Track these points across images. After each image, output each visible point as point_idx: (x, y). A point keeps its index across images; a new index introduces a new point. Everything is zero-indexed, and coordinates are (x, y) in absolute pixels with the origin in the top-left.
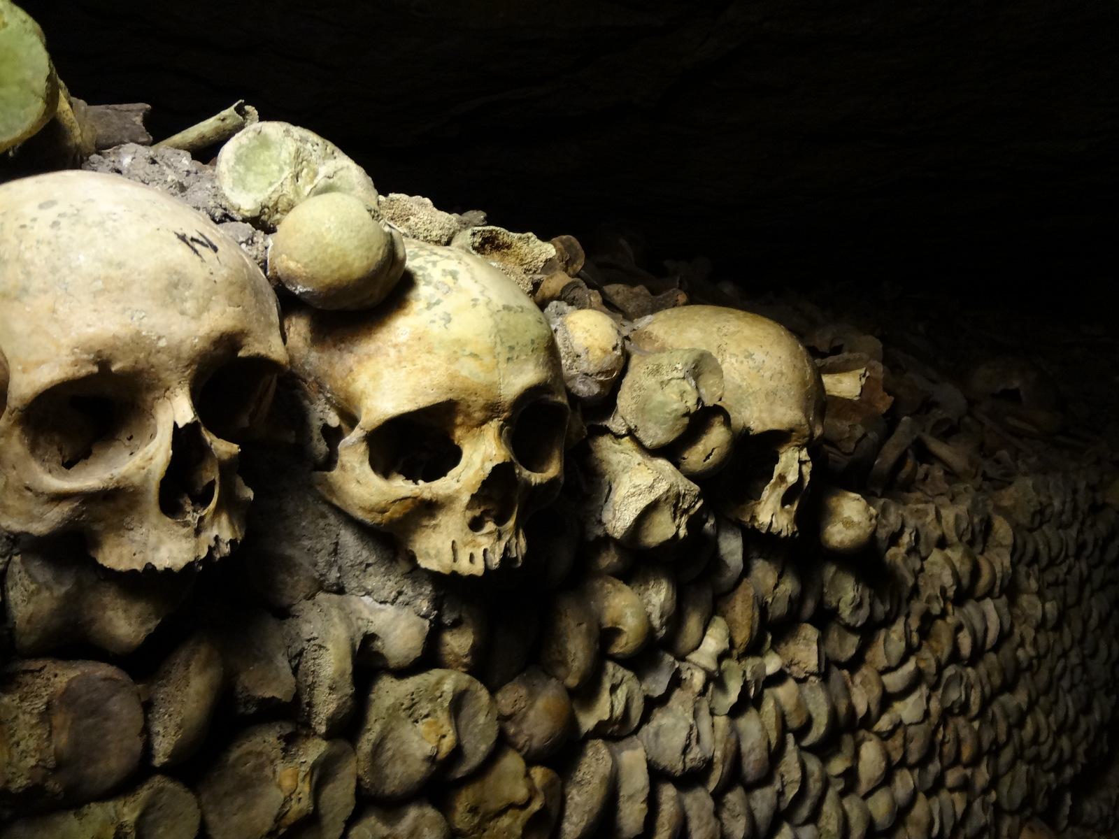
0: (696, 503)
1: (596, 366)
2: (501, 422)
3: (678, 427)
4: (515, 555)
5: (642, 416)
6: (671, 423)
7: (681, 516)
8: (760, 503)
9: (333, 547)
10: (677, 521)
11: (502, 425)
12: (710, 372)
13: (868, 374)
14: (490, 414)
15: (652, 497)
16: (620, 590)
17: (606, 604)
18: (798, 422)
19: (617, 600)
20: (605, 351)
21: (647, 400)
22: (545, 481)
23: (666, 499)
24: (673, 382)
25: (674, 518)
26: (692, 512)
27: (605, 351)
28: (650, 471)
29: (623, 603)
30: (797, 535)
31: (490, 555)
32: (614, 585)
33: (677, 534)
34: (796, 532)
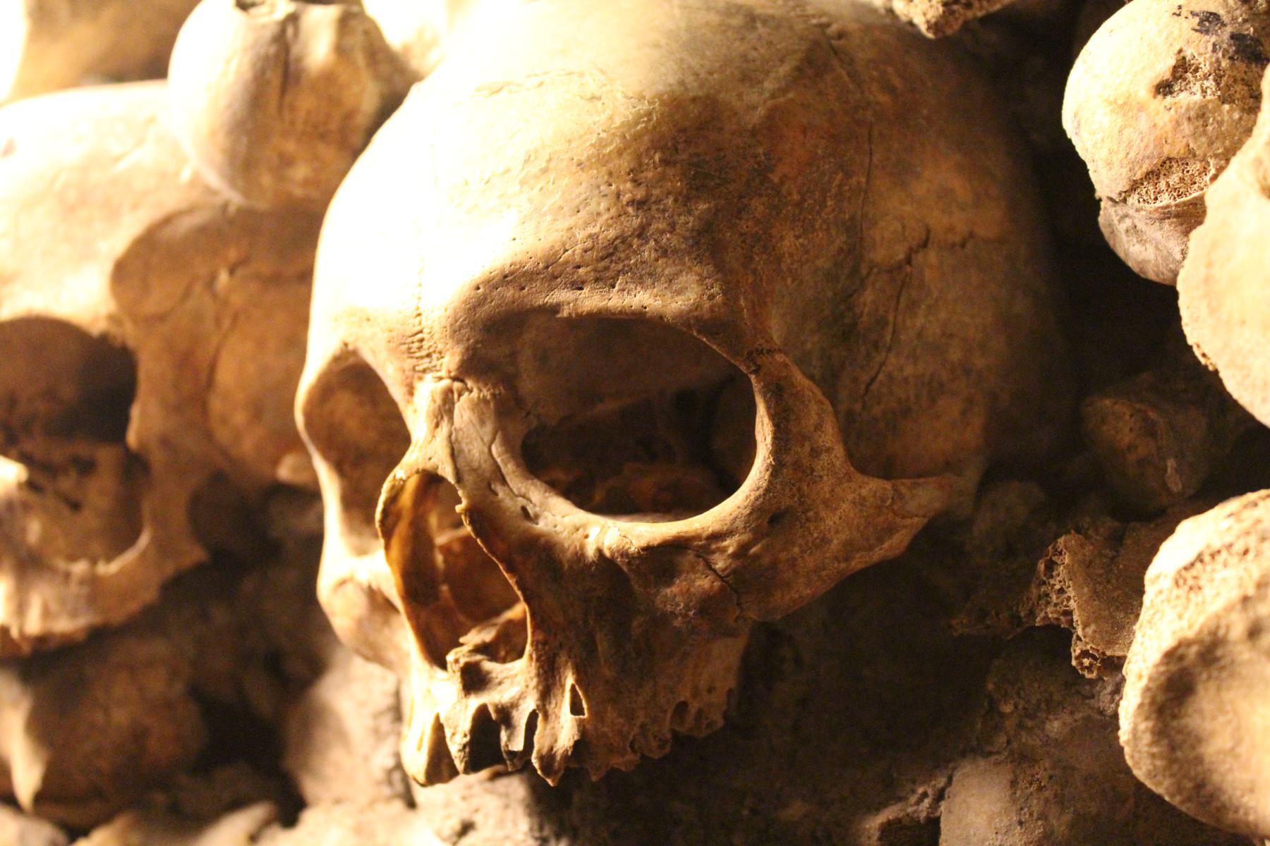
2: (446, 382)
4: (518, 745)
5: (1213, 310)
9: (389, 701)
11: (449, 391)
14: (409, 363)
22: (635, 545)
31: (448, 732)
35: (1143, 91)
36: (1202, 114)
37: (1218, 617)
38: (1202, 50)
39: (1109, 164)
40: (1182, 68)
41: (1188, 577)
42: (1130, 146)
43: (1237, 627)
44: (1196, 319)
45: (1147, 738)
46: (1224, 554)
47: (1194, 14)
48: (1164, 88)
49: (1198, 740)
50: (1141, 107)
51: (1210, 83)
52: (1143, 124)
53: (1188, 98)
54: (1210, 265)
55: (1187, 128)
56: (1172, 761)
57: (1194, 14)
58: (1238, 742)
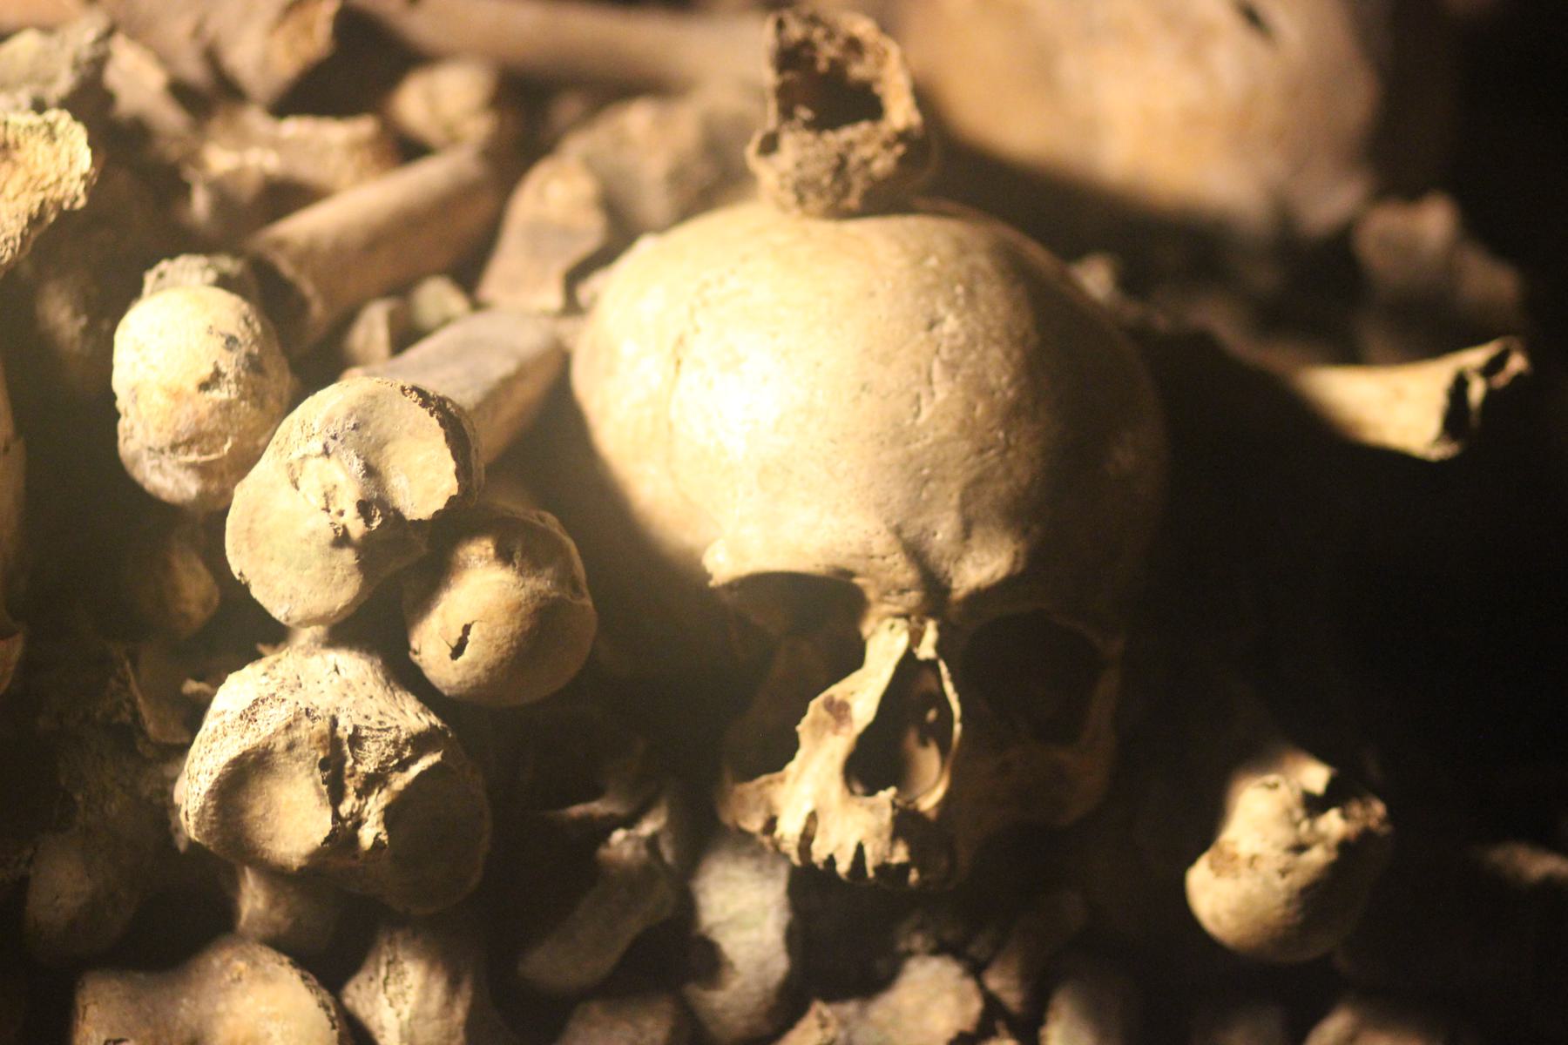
0: (403, 766)
1: (160, 430)
3: (339, 573)
5: (251, 549)
6: (319, 563)
7: (363, 792)
8: (782, 780)
10: (345, 808)
12: (411, 433)
13: (1517, 363)
15: (249, 740)
16: (268, 979)
17: (221, 1007)
18: (856, 549)
19: (250, 1000)
20: (176, 395)
21: (256, 509)
23: (290, 747)
24: (311, 464)
25: (336, 796)
26: (400, 781)
27: (176, 395)
28: (266, 679)
29: (263, 1009)
30: (914, 876)
32: (255, 964)
33: (343, 836)
34: (903, 869)
35: (191, 387)
36: (227, 407)
37: (270, 737)
38: (230, 364)
39: (160, 430)
40: (216, 378)
41: (249, 716)
42: (178, 420)
43: (281, 743)
44: (238, 552)
45: (211, 811)
46: (270, 700)
47: (222, 335)
48: (204, 386)
49: (243, 811)
50: (189, 398)
51: (233, 386)
52: (189, 409)
53: (221, 394)
54: (252, 521)
55: (218, 415)
56: (222, 824)
57: (222, 335)
58: (268, 810)
